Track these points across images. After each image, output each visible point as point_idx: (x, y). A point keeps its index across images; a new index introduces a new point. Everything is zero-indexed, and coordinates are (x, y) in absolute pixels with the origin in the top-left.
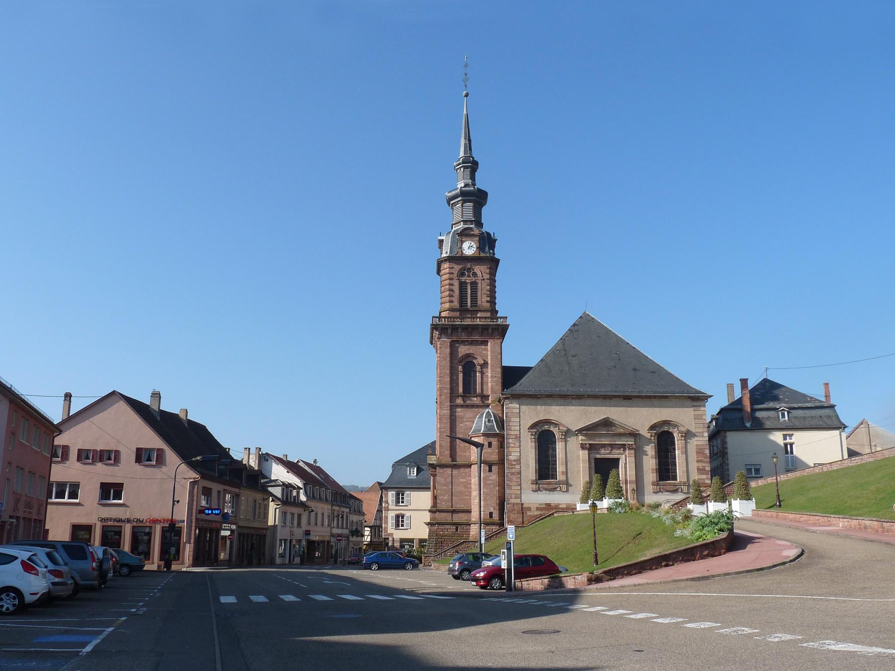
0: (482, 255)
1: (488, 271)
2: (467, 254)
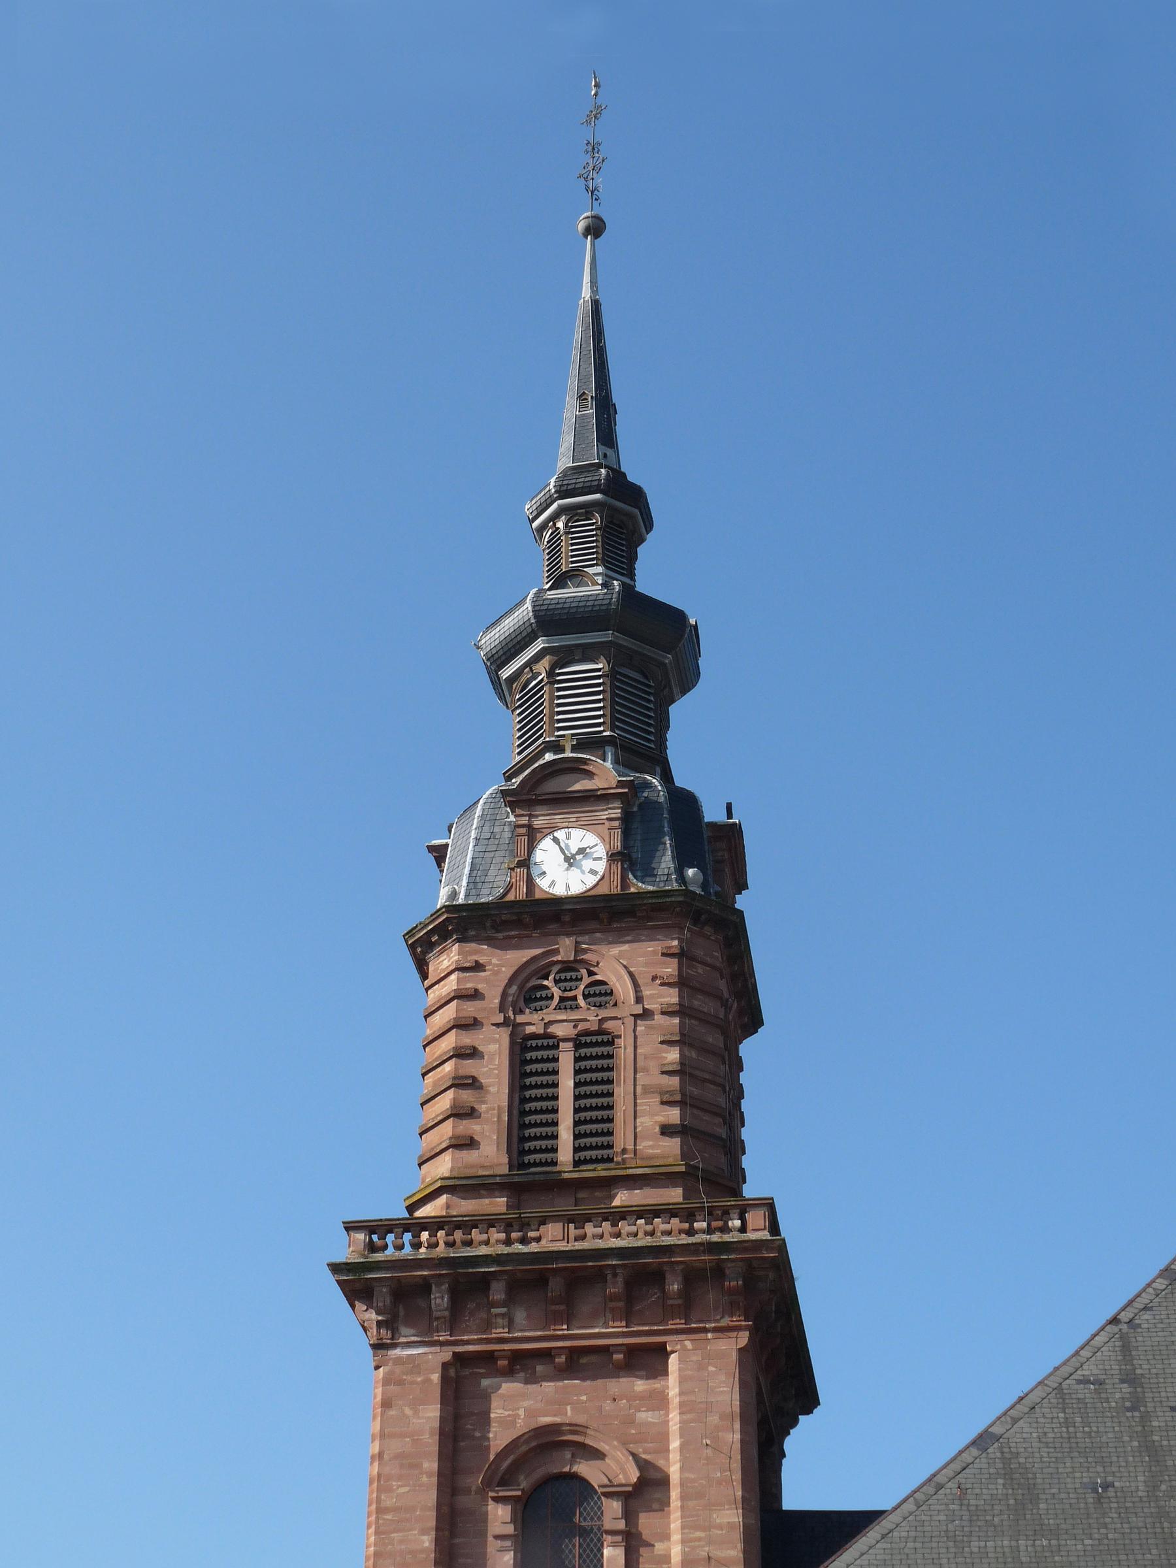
0: (637, 886)
1: (670, 969)
2: (559, 891)
